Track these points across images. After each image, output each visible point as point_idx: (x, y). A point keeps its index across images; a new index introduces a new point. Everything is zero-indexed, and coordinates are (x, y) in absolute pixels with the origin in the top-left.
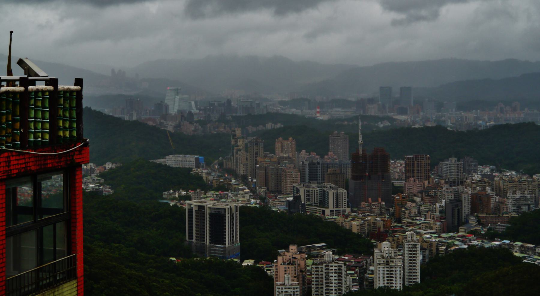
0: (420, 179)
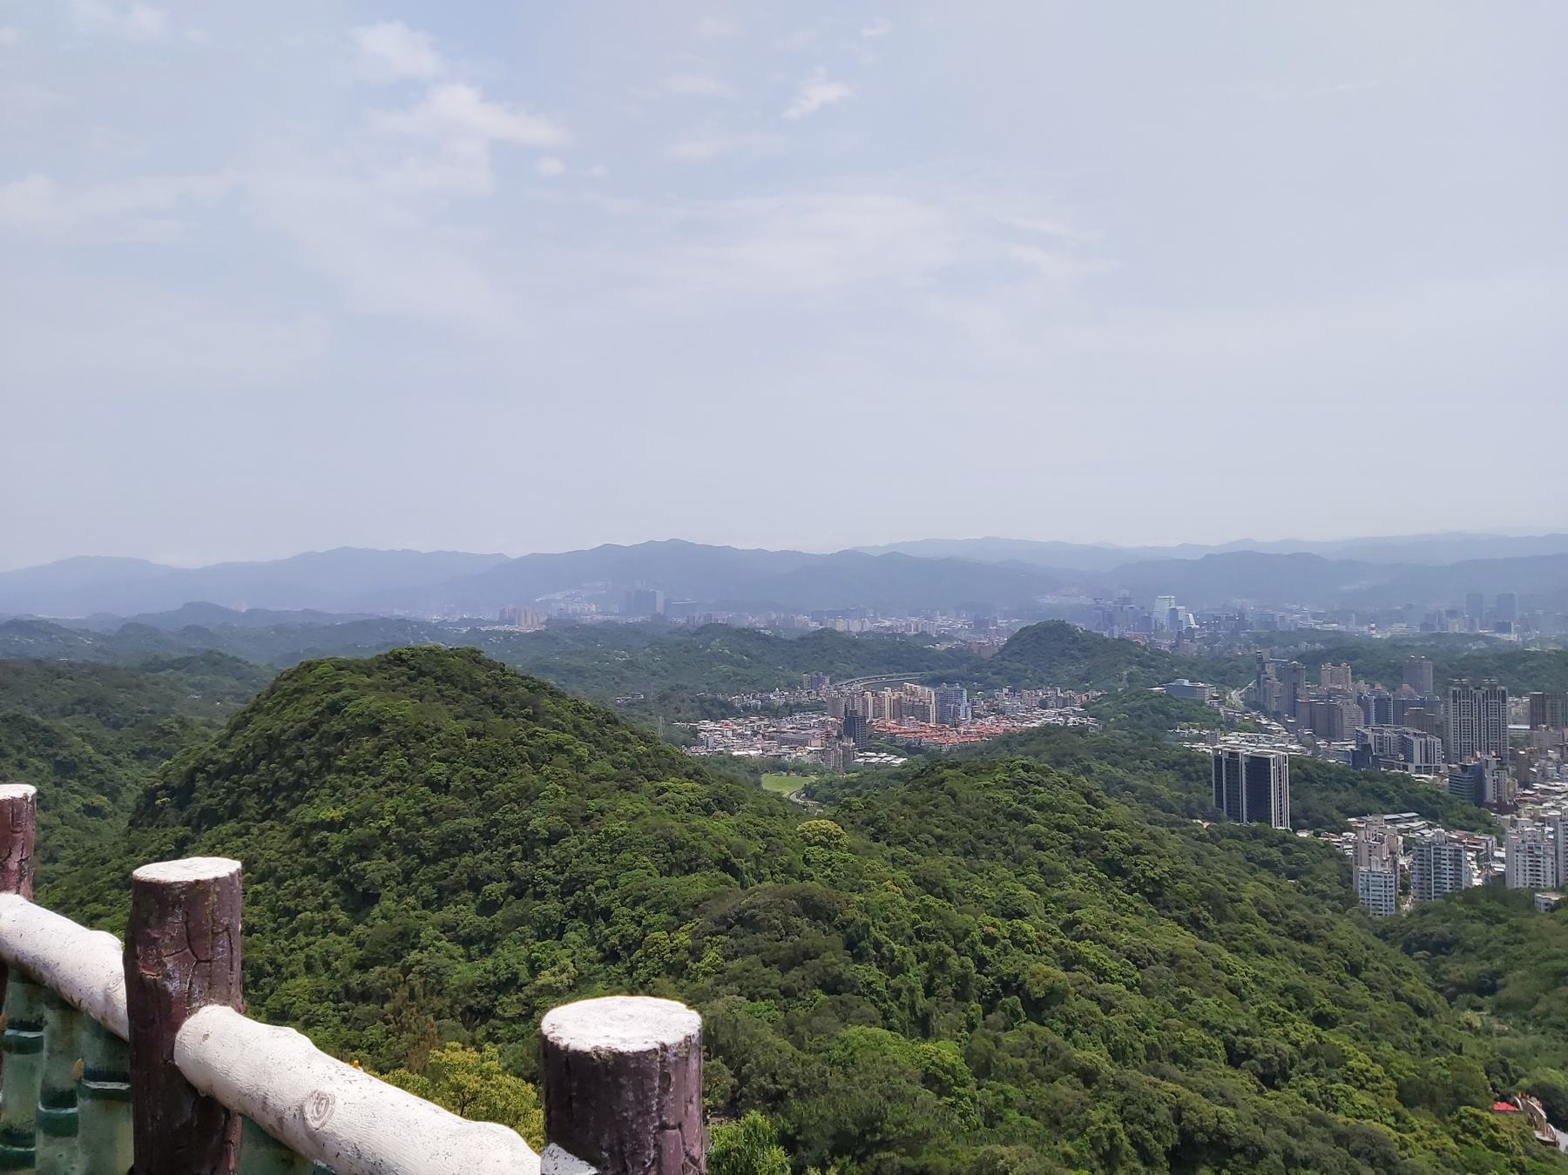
0: (1554, 725)
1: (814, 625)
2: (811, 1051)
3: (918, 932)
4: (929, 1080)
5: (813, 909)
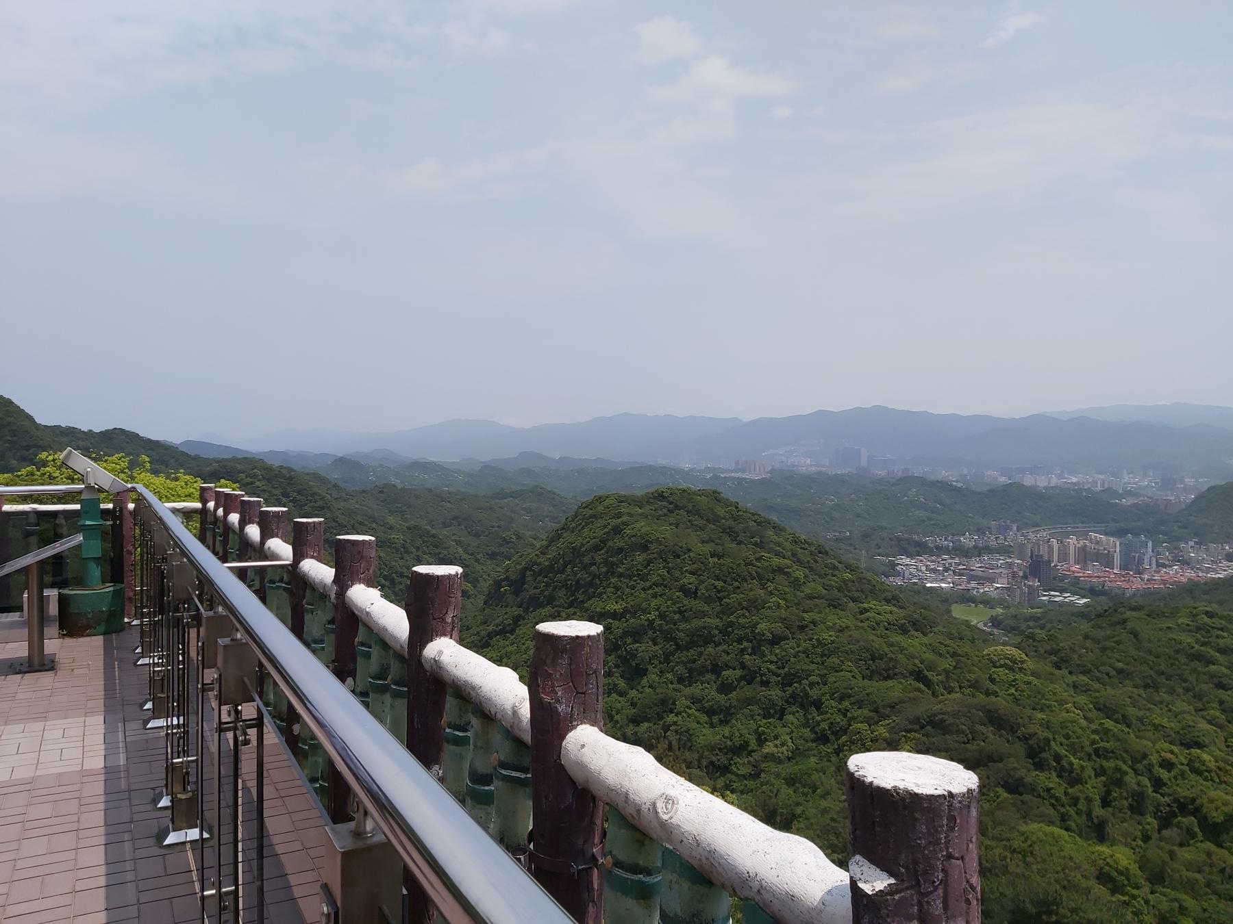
1: (1003, 480)
2: (993, 838)
3: (1097, 751)
4: (1103, 877)
5: (998, 721)
